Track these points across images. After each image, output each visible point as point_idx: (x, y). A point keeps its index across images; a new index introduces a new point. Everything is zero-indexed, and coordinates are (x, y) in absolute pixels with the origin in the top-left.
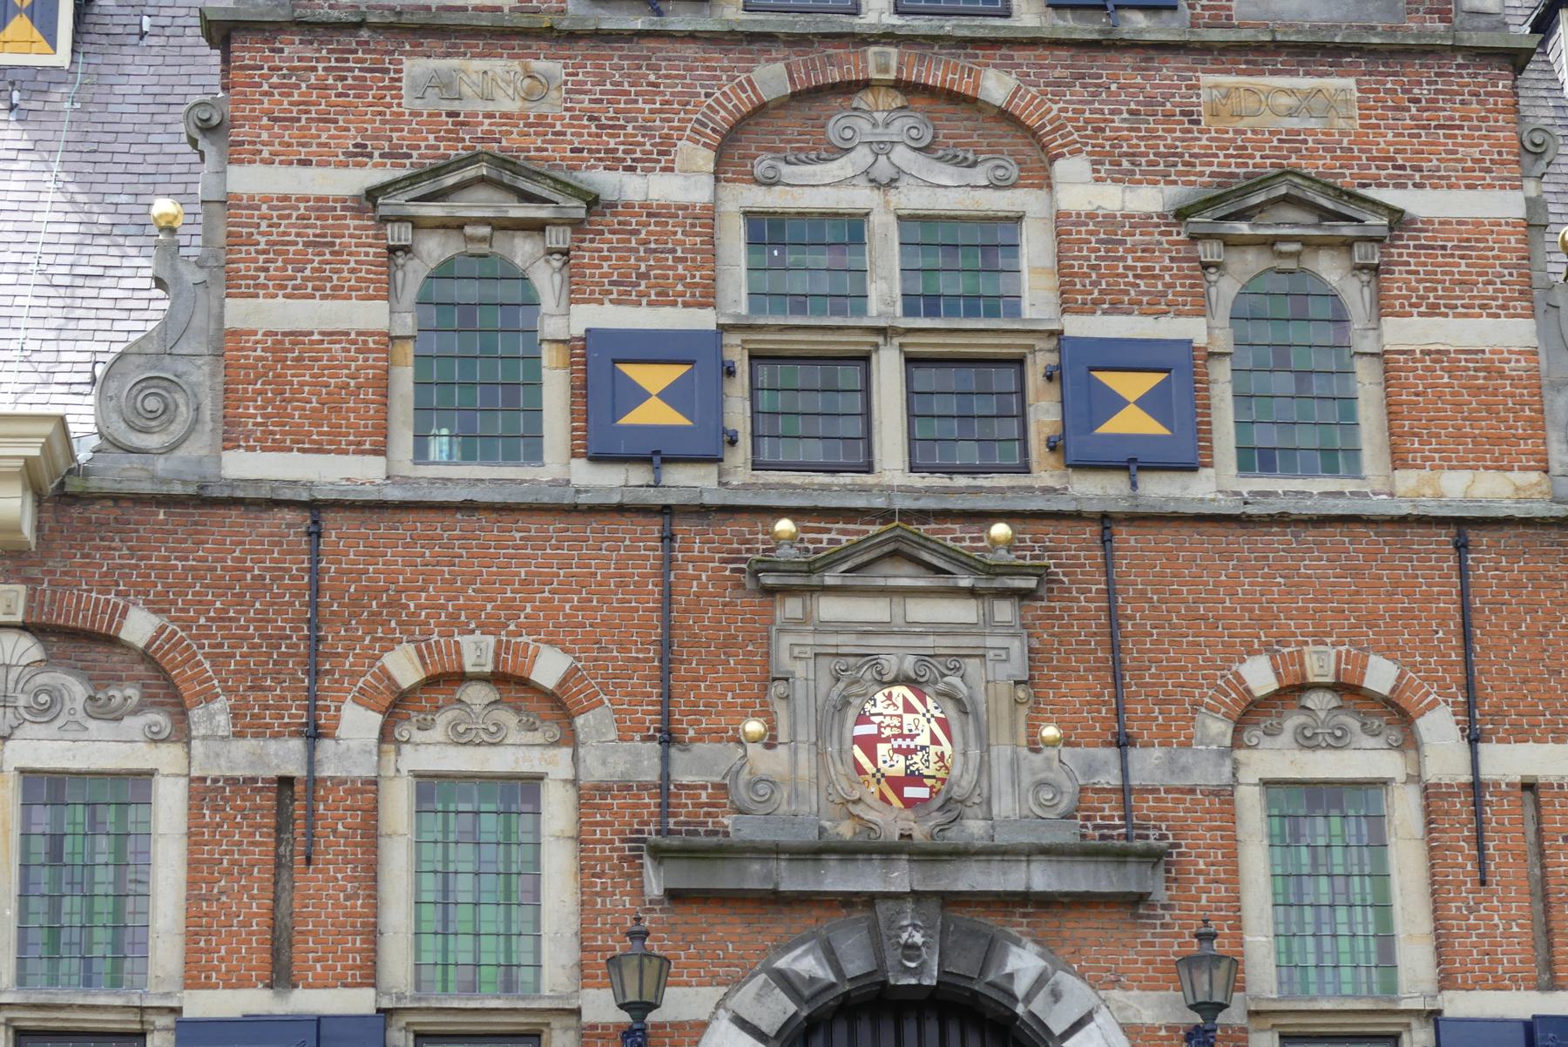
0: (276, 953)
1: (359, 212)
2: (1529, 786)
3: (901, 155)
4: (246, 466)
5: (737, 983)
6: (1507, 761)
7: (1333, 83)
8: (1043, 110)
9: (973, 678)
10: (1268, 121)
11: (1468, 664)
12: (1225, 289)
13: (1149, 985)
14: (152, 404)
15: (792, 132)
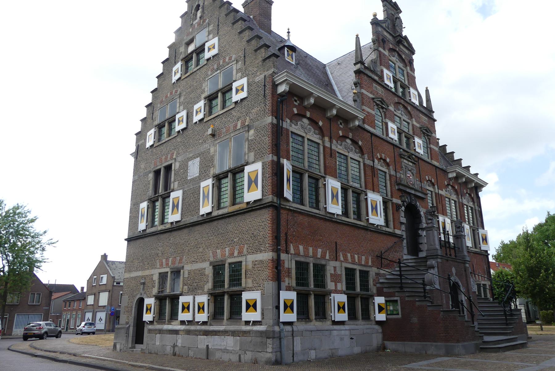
4: (367, 127)
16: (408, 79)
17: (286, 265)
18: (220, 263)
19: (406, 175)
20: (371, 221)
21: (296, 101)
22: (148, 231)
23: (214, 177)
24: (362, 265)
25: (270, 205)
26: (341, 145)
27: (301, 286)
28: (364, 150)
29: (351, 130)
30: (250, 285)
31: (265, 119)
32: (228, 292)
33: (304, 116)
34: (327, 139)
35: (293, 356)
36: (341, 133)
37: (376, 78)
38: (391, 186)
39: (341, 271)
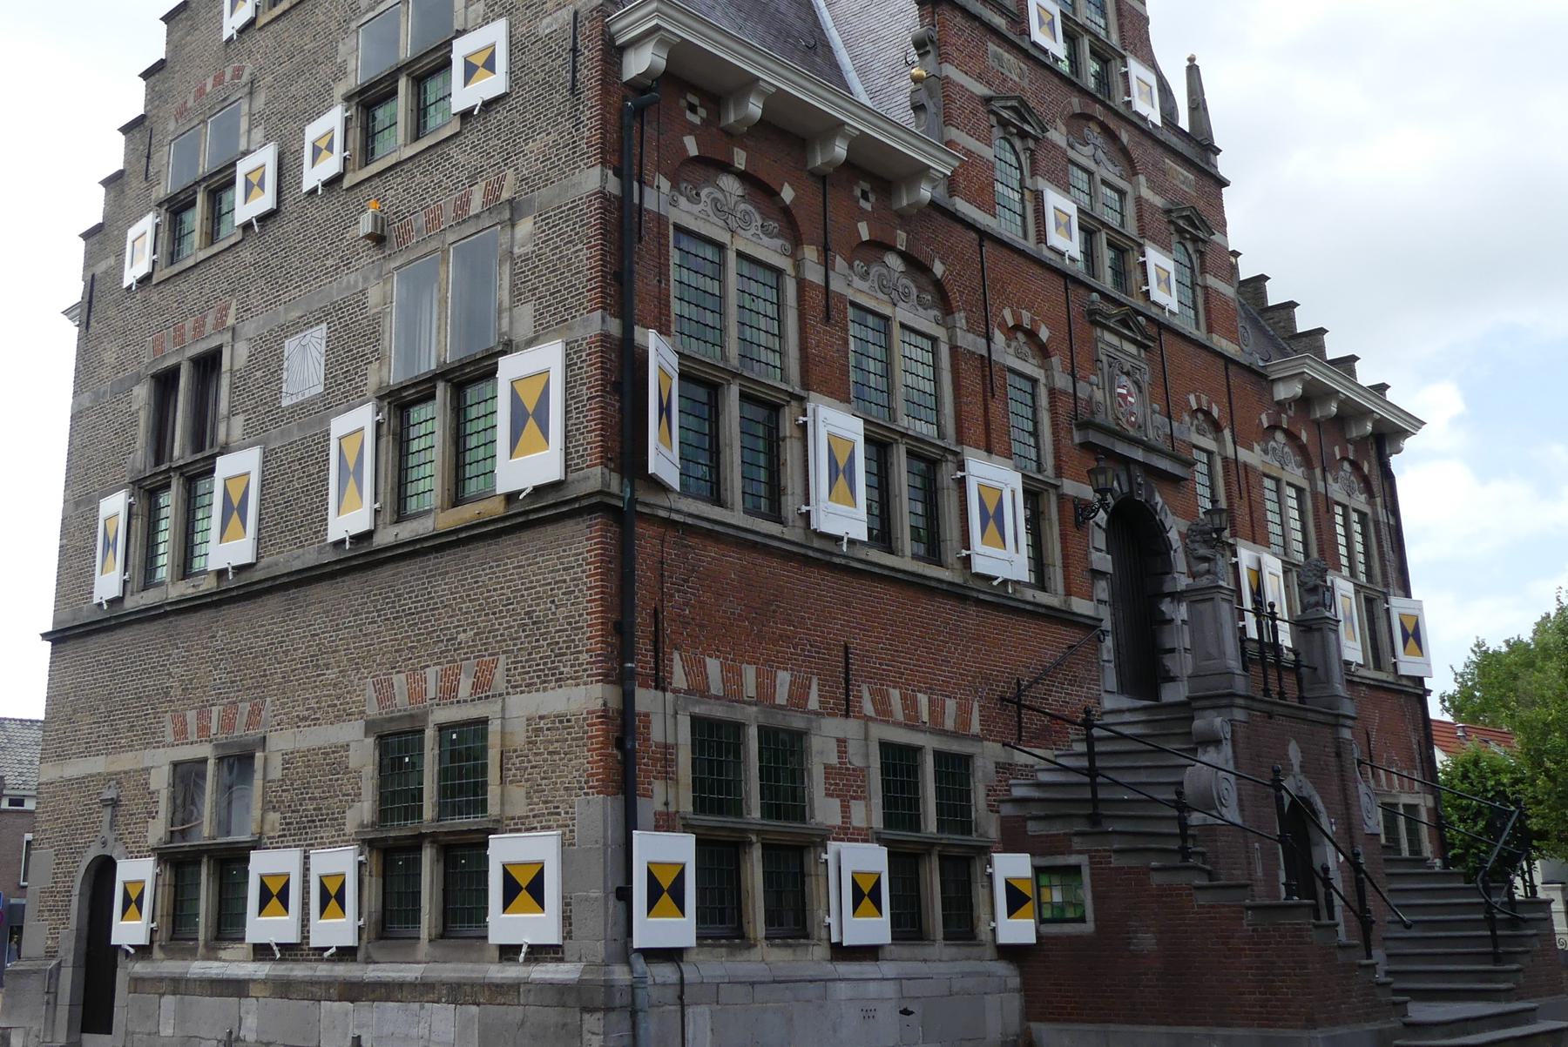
2: (1246, 465)
8: (1136, 154)
16: (1121, 27)
17: (656, 734)
18: (406, 726)
19: (1112, 390)
20: (979, 566)
21: (693, 108)
22: (131, 603)
23: (380, 398)
24: (944, 733)
25: (597, 506)
26: (865, 276)
27: (711, 812)
28: (954, 296)
29: (904, 218)
30: (518, 807)
31: (575, 179)
32: (433, 837)
33: (726, 167)
34: (810, 253)
36: (864, 232)
37: (999, 21)
38: (1055, 433)
39: (867, 756)
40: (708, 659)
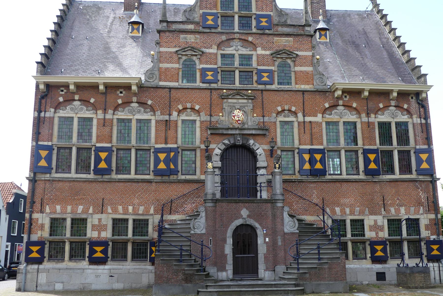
0: (165, 140)
1: (175, 53)
2: (310, 122)
3: (239, 47)
4: (162, 83)
5: (218, 144)
6: (308, 119)
7: (290, 39)
9: (246, 109)
10: (282, 43)
11: (304, 108)
12: (277, 63)
13: (266, 144)
14: (151, 76)
15: (226, 44)
17: (40, 222)
21: (62, 91)
26: (123, 111)
29: (135, 94)
34: (100, 112)
35: (37, 286)
39: (107, 222)
40: (57, 206)
